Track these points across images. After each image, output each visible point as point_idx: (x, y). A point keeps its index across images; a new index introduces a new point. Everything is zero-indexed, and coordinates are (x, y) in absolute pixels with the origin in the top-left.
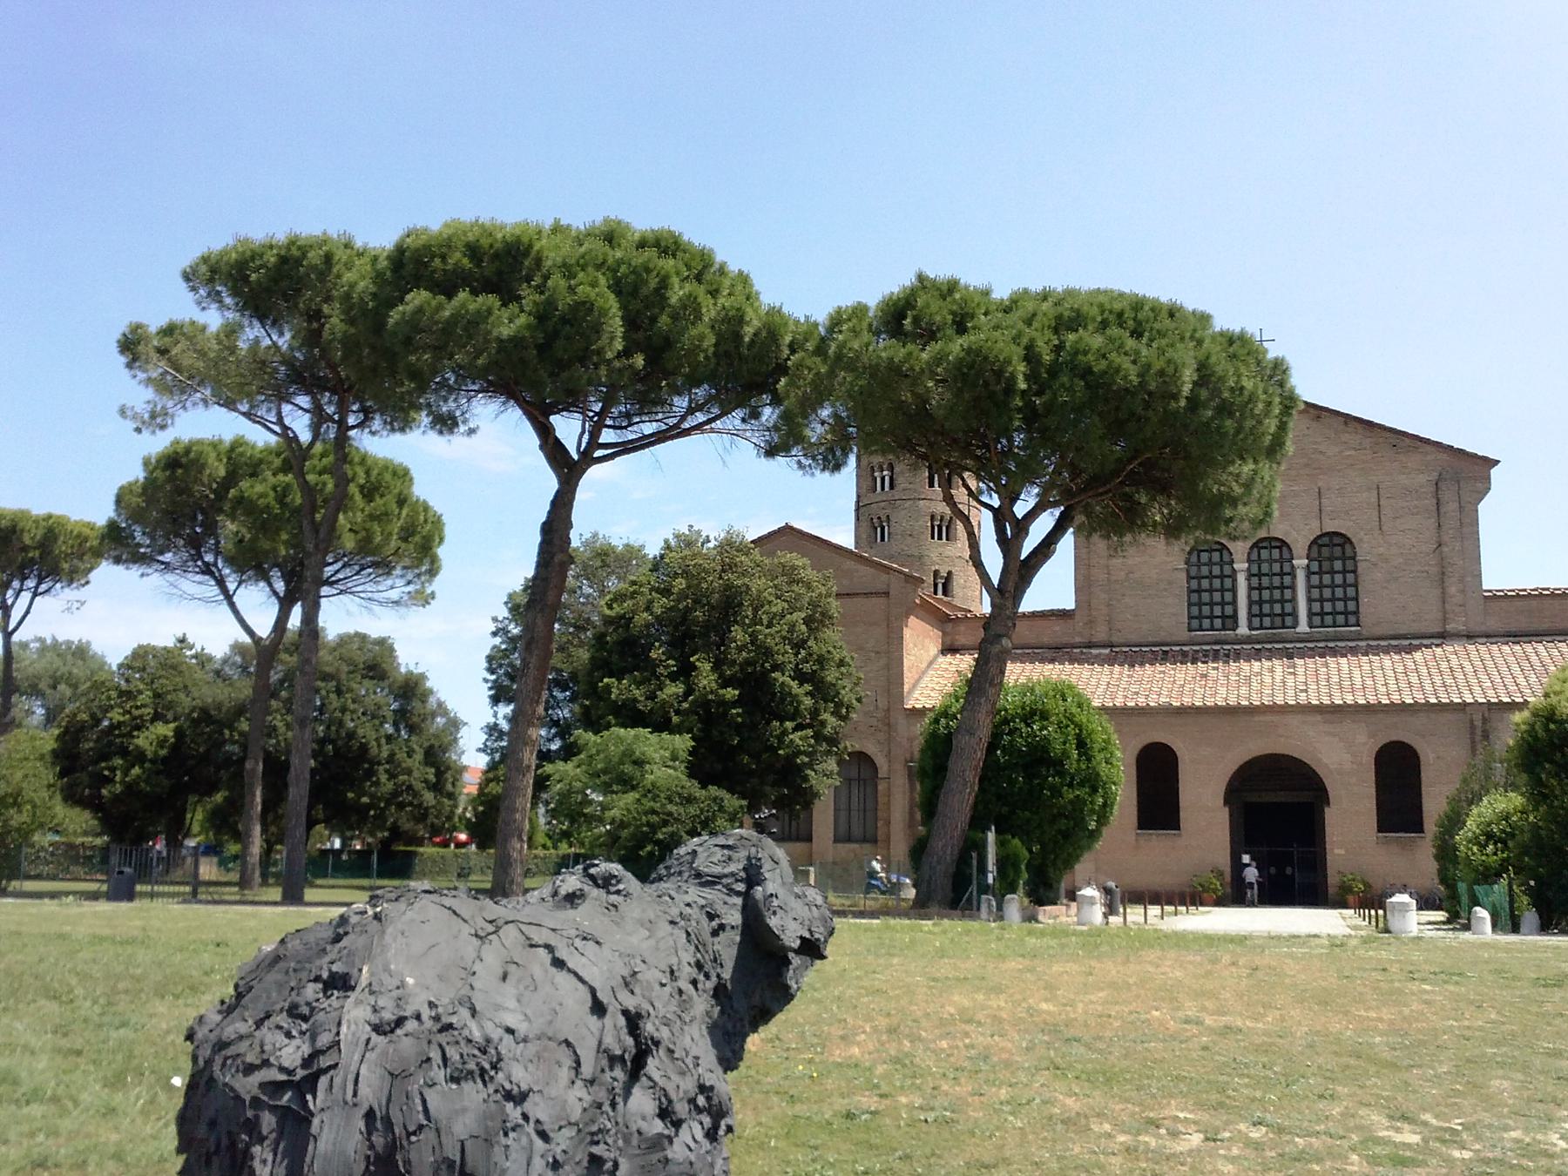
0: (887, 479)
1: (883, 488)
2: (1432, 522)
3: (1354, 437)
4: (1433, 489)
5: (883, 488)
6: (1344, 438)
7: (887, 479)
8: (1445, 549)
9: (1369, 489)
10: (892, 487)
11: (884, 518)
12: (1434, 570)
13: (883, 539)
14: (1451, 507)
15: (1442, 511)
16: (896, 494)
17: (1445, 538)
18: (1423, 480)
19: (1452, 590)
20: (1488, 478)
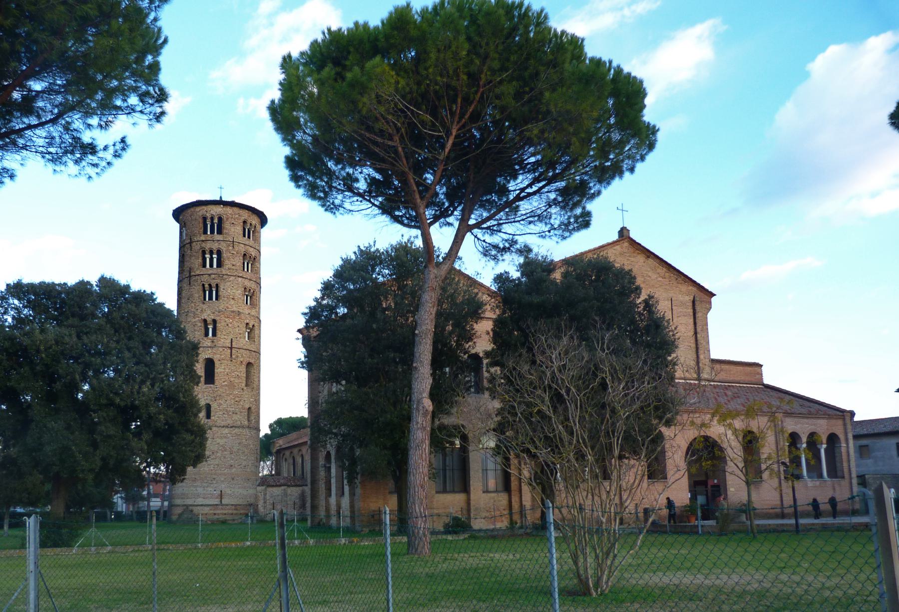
0: (215, 260)
1: (211, 265)
2: (692, 320)
3: (662, 270)
4: (691, 304)
5: (211, 265)
6: (659, 271)
7: (215, 260)
8: (698, 336)
9: (668, 300)
10: (219, 265)
11: (214, 285)
12: (694, 345)
13: (211, 298)
14: (699, 315)
15: (697, 316)
16: (224, 271)
17: (699, 330)
18: (688, 299)
19: (702, 357)
20: (710, 303)
